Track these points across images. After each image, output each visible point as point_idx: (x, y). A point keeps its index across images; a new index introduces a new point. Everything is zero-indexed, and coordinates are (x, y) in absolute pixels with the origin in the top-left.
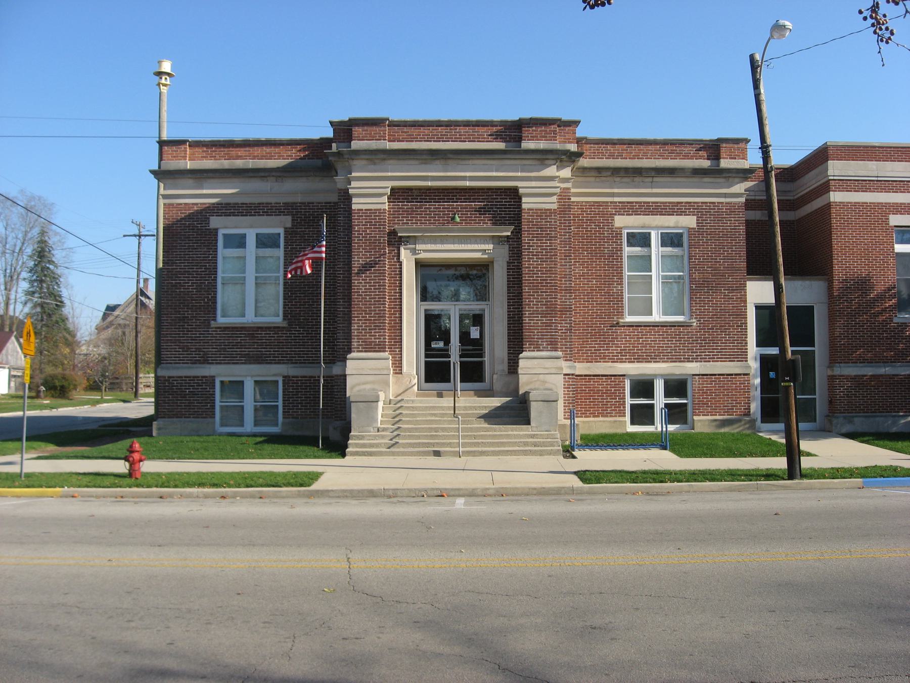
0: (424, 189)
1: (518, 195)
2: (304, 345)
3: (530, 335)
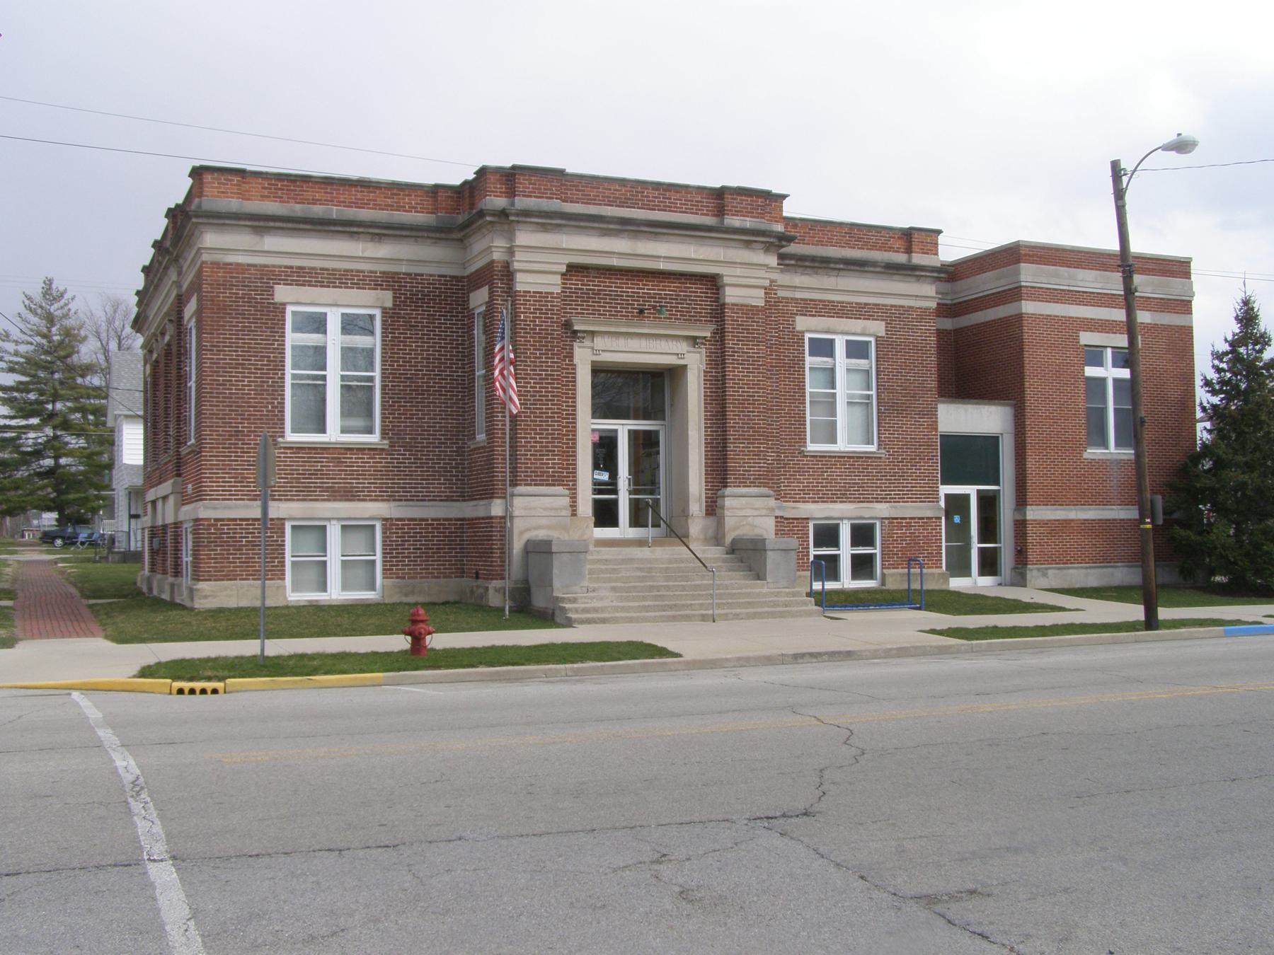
0: (603, 269)
1: (716, 286)
2: (412, 475)
3: (736, 467)
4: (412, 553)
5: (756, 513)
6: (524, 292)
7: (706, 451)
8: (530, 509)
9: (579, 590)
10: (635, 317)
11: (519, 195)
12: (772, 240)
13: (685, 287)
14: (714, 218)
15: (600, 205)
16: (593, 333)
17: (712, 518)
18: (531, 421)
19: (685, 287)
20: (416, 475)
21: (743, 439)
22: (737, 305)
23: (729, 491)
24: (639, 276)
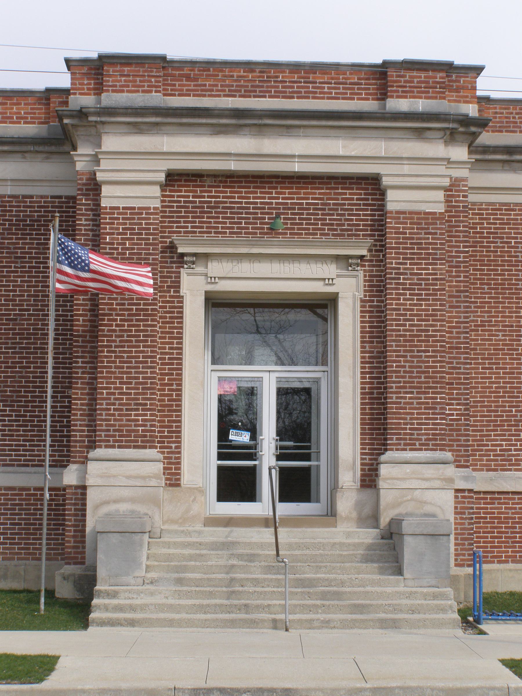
0: (223, 176)
1: (379, 189)
2: (12, 435)
3: (400, 424)
4: (9, 529)
5: (426, 485)
6: (111, 208)
7: (362, 404)
8: (109, 477)
9: (132, 581)
10: (266, 234)
11: (108, 91)
12: (451, 126)
13: (335, 194)
14: (376, 102)
15: (219, 96)
16: (207, 256)
17: (369, 491)
18: (116, 367)
19: (335, 194)
20: (18, 436)
21: (410, 387)
22: (404, 213)
23: (389, 455)
24: (271, 183)
